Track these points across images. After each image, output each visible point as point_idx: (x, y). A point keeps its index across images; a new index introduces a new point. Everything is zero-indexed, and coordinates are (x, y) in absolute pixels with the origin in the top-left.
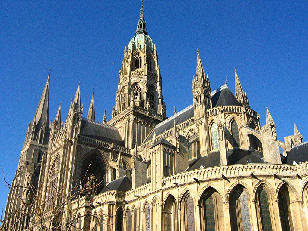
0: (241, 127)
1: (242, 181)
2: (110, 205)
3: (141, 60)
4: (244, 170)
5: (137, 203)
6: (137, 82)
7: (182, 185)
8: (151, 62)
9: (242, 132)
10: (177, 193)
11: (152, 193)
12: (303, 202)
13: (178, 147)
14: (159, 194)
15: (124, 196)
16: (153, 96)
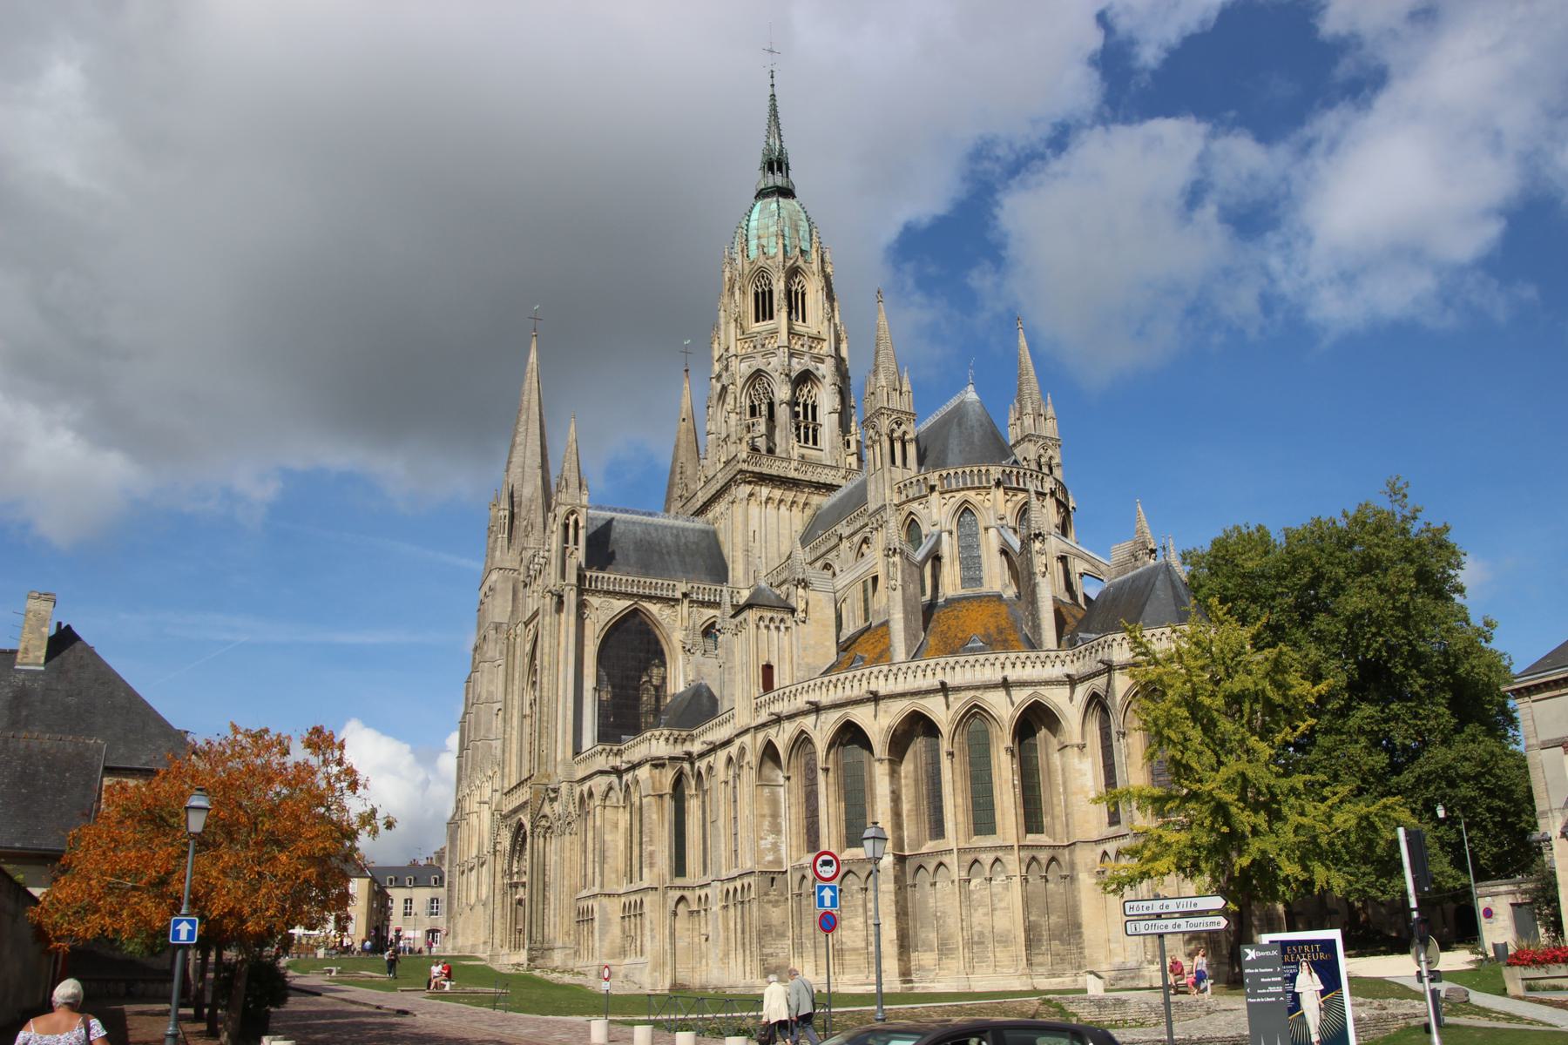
0: (986, 529)
1: (922, 702)
2: (655, 766)
3: (771, 292)
4: (929, 672)
5: (711, 759)
6: (759, 370)
7: (791, 717)
8: (803, 295)
9: (988, 544)
10: (781, 738)
11: (738, 735)
12: (1084, 746)
13: (801, 606)
14: (747, 738)
15: (692, 738)
16: (814, 408)
